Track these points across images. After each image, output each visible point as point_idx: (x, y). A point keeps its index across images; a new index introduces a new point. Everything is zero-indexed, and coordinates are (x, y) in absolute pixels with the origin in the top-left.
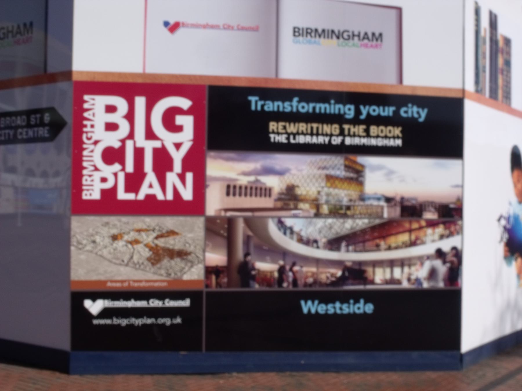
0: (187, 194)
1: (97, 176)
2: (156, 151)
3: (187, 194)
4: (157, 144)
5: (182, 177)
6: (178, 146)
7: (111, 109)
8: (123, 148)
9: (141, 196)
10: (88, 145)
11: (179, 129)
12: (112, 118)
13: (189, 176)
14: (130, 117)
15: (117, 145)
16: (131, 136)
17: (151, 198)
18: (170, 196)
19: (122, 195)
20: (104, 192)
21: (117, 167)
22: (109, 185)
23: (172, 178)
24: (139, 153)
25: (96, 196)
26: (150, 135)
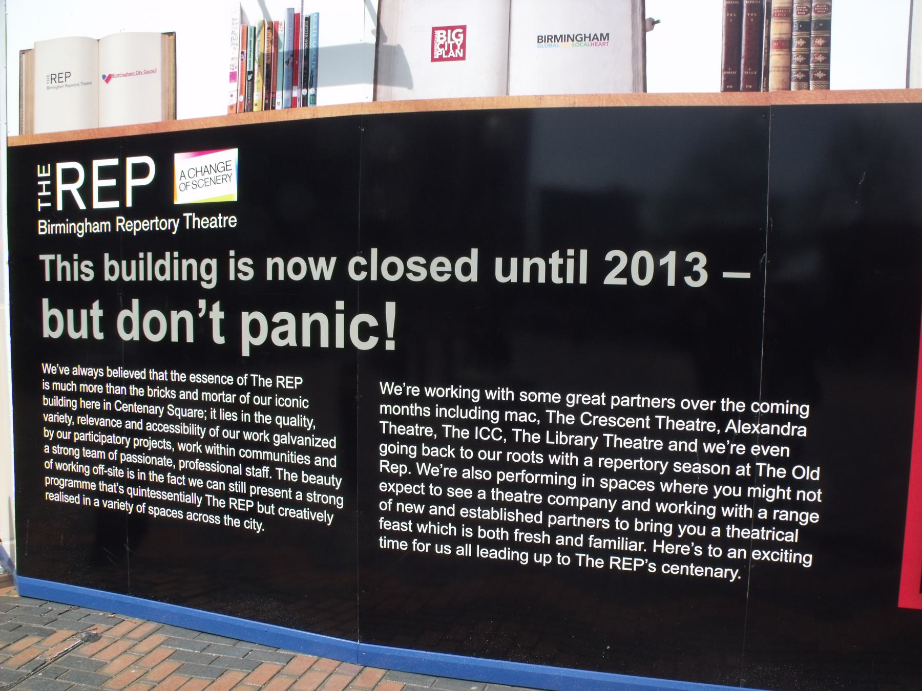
0: (461, 55)
1: (438, 52)
2: (453, 44)
3: (461, 55)
4: (453, 42)
5: (460, 51)
6: (459, 42)
7: (442, 34)
8: (445, 44)
9: (449, 57)
10: (436, 44)
11: (459, 38)
12: (442, 36)
13: (462, 50)
14: (447, 36)
15: (443, 43)
16: (447, 40)
17: (451, 57)
18: (457, 56)
19: (444, 56)
20: (439, 56)
21: (443, 49)
22: (441, 54)
23: (457, 51)
24: (449, 45)
25: (438, 57)
26: (452, 40)
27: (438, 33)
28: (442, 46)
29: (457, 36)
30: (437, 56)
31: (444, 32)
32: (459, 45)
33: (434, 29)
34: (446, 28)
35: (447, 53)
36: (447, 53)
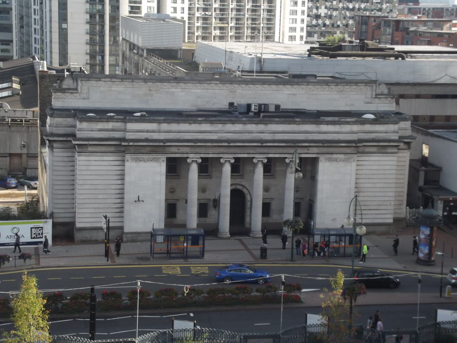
3: (42, 237)
14: (36, 230)
19: (36, 237)
23: (40, 235)
24: (37, 233)
26: (38, 232)
27: (33, 229)
28: (34, 234)
29: (40, 230)
30: (33, 237)
31: (35, 229)
32: (41, 233)
33: (31, 228)
34: (36, 228)
35: (37, 236)
36: (37, 236)
